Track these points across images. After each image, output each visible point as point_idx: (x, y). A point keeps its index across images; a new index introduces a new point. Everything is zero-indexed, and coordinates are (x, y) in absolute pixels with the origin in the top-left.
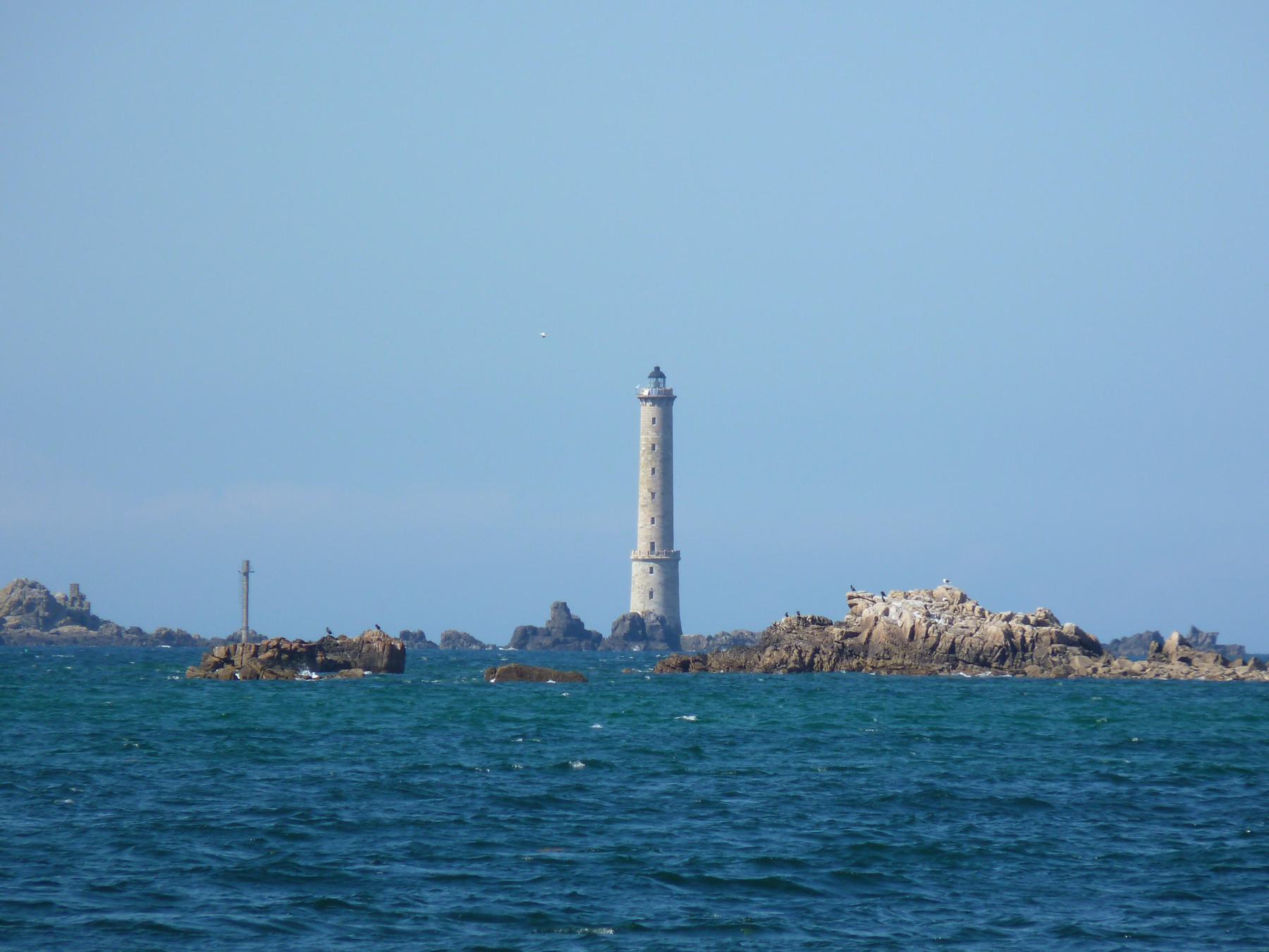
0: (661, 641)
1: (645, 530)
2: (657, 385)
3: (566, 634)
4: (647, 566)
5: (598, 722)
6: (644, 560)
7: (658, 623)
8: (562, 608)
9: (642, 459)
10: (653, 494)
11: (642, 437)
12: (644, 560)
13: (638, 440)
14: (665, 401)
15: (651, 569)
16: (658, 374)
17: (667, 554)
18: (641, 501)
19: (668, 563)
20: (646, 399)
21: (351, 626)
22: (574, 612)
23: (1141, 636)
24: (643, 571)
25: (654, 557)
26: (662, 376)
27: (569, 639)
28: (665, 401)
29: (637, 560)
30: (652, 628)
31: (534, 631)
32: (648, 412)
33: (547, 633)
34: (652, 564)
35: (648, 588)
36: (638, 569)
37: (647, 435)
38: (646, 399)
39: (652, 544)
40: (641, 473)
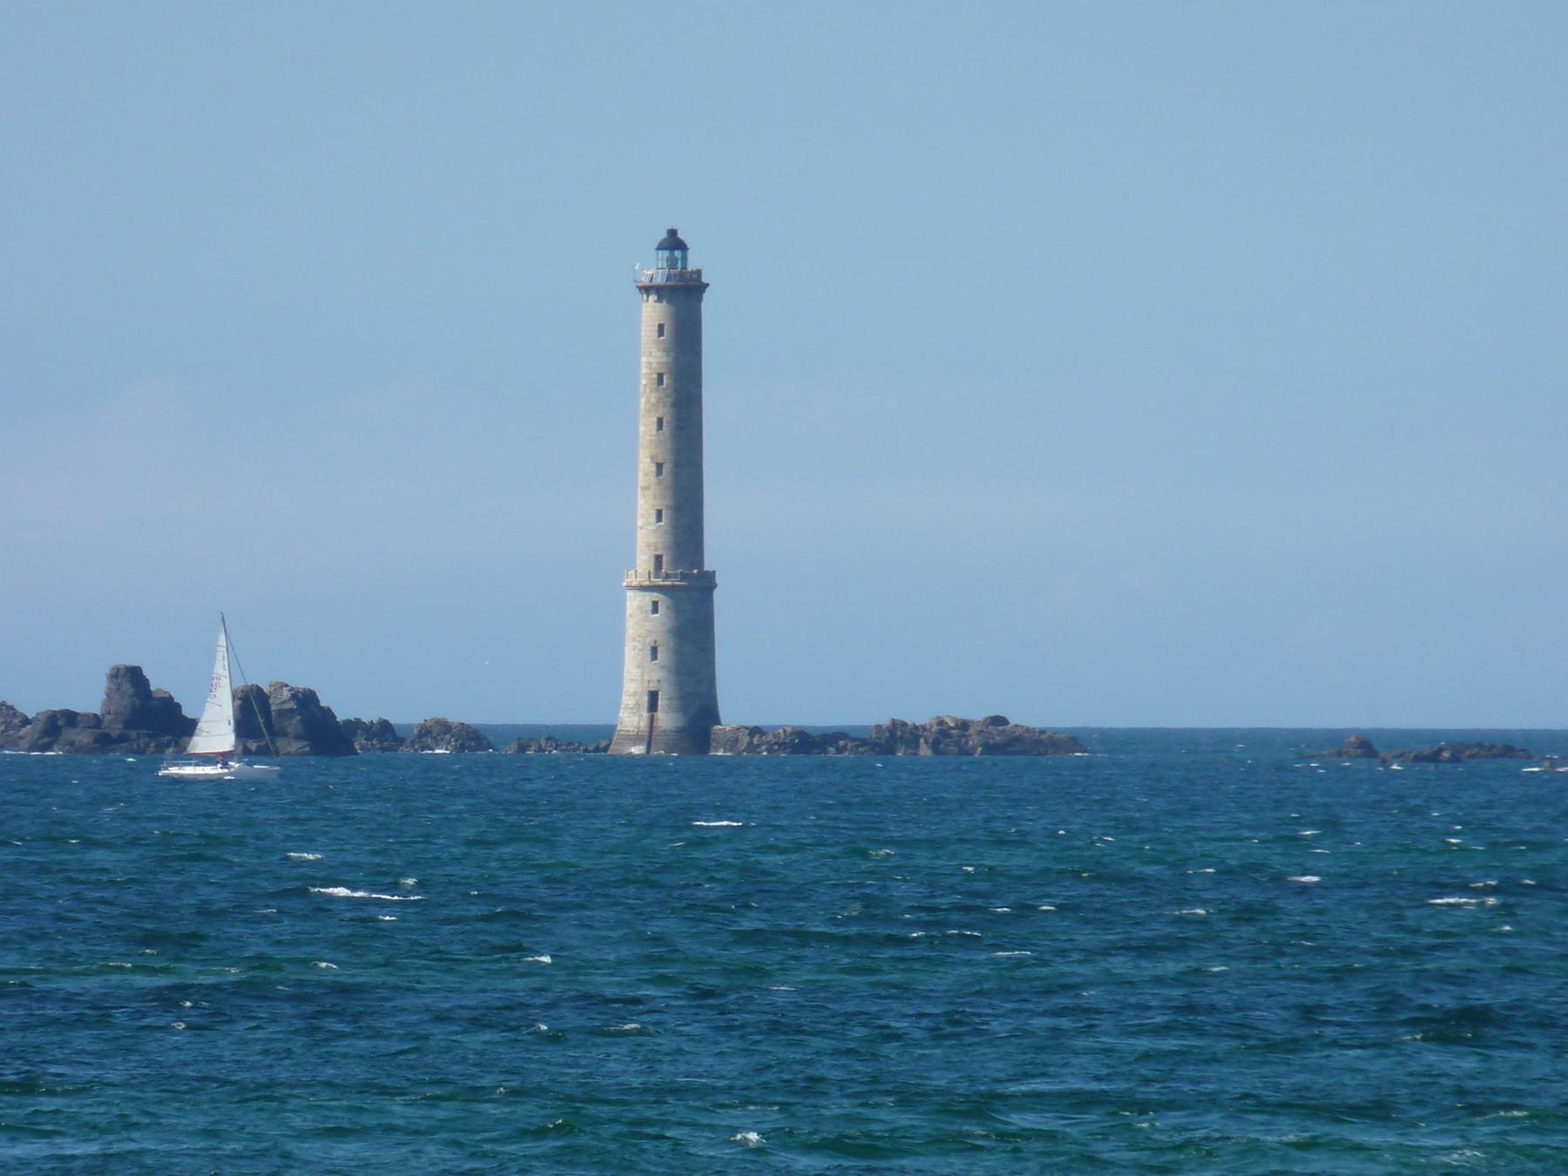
0: (298, 738)
1: (646, 536)
2: (672, 263)
3: (130, 724)
4: (648, 598)
5: (1507, 923)
6: (642, 588)
7: (292, 705)
8: (133, 677)
9: (643, 400)
10: (659, 466)
11: (644, 360)
12: (642, 588)
13: (639, 363)
14: (683, 293)
15: (655, 604)
16: (674, 243)
17: (684, 577)
18: (642, 480)
19: (689, 593)
20: (647, 290)
21: (919, 714)
22: (158, 682)
23: (905, 724)
24: (641, 608)
25: (659, 582)
26: (681, 246)
27: (133, 733)
28: (683, 293)
29: (630, 587)
30: (281, 712)
31: (71, 718)
32: (652, 312)
33: (96, 721)
34: (656, 596)
35: (650, 640)
36: (635, 603)
37: (650, 356)
38: (647, 290)
39: (658, 559)
40: (642, 429)
